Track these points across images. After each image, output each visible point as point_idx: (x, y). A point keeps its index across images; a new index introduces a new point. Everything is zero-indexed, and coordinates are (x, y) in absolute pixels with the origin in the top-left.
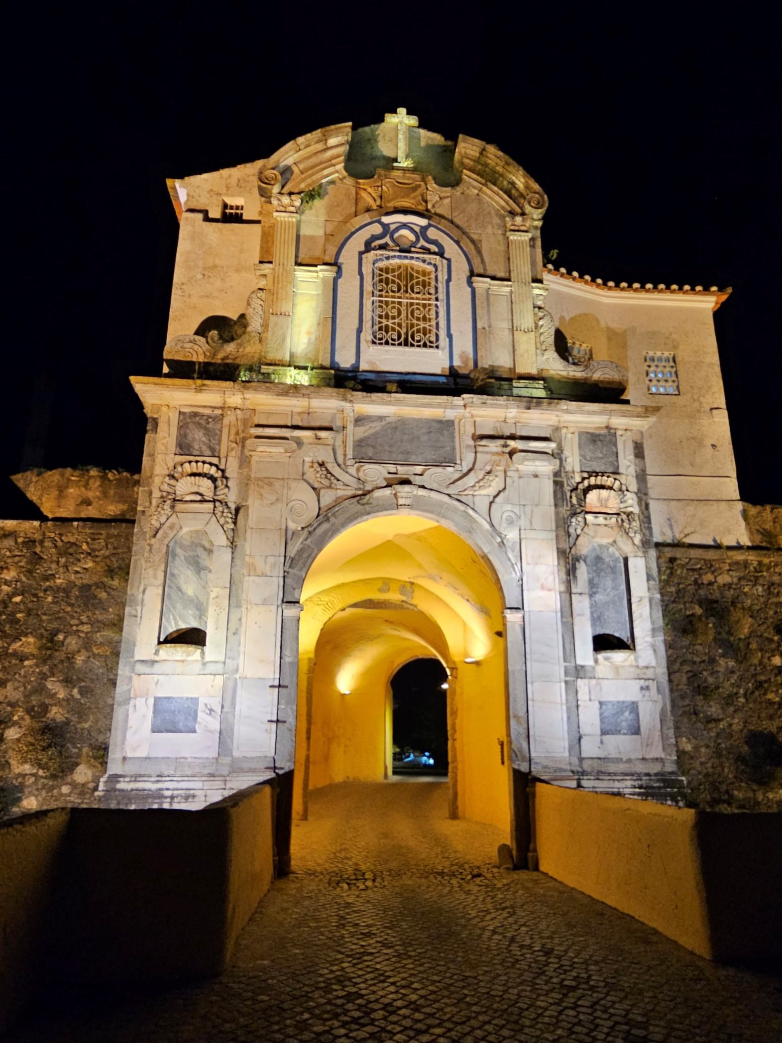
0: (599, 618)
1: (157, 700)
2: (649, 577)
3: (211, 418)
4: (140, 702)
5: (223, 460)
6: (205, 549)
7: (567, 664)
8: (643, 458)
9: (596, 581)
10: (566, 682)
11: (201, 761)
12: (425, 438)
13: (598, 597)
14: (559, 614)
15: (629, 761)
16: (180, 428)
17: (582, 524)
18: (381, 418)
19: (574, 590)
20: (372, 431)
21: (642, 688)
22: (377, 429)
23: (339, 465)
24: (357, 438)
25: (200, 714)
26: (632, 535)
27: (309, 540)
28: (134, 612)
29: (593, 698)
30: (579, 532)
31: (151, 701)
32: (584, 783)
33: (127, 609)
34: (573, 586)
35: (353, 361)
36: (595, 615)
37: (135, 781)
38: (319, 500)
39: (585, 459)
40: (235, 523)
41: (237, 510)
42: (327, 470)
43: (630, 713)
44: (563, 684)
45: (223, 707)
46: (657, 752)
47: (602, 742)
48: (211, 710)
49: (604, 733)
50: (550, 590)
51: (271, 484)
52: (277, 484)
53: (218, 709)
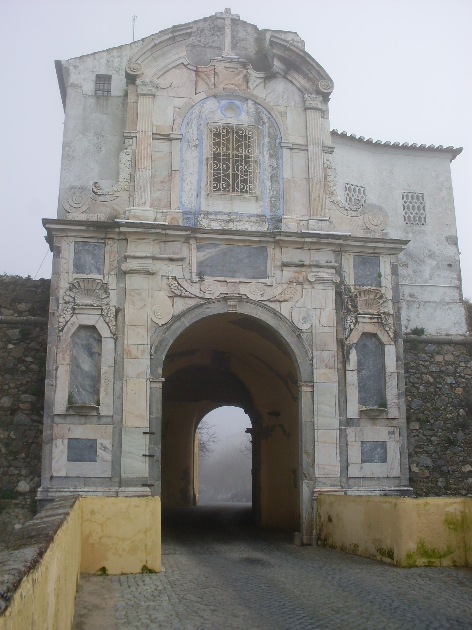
2: (398, 359)
3: (96, 246)
4: (59, 442)
5: (106, 277)
6: (95, 339)
7: (341, 418)
9: (363, 361)
10: (340, 430)
11: (100, 479)
13: (364, 372)
14: (337, 384)
16: (75, 253)
17: (354, 321)
19: (348, 368)
20: (210, 255)
22: (213, 254)
23: (186, 280)
25: (98, 450)
27: (167, 334)
28: (51, 382)
29: (357, 440)
30: (352, 327)
31: (66, 441)
33: (47, 381)
34: (347, 365)
36: (361, 385)
37: (60, 491)
38: (173, 305)
39: (358, 276)
41: (117, 312)
43: (381, 449)
44: (338, 431)
45: (113, 446)
46: (396, 472)
47: (361, 468)
49: (363, 461)
50: (331, 368)
53: (110, 447)
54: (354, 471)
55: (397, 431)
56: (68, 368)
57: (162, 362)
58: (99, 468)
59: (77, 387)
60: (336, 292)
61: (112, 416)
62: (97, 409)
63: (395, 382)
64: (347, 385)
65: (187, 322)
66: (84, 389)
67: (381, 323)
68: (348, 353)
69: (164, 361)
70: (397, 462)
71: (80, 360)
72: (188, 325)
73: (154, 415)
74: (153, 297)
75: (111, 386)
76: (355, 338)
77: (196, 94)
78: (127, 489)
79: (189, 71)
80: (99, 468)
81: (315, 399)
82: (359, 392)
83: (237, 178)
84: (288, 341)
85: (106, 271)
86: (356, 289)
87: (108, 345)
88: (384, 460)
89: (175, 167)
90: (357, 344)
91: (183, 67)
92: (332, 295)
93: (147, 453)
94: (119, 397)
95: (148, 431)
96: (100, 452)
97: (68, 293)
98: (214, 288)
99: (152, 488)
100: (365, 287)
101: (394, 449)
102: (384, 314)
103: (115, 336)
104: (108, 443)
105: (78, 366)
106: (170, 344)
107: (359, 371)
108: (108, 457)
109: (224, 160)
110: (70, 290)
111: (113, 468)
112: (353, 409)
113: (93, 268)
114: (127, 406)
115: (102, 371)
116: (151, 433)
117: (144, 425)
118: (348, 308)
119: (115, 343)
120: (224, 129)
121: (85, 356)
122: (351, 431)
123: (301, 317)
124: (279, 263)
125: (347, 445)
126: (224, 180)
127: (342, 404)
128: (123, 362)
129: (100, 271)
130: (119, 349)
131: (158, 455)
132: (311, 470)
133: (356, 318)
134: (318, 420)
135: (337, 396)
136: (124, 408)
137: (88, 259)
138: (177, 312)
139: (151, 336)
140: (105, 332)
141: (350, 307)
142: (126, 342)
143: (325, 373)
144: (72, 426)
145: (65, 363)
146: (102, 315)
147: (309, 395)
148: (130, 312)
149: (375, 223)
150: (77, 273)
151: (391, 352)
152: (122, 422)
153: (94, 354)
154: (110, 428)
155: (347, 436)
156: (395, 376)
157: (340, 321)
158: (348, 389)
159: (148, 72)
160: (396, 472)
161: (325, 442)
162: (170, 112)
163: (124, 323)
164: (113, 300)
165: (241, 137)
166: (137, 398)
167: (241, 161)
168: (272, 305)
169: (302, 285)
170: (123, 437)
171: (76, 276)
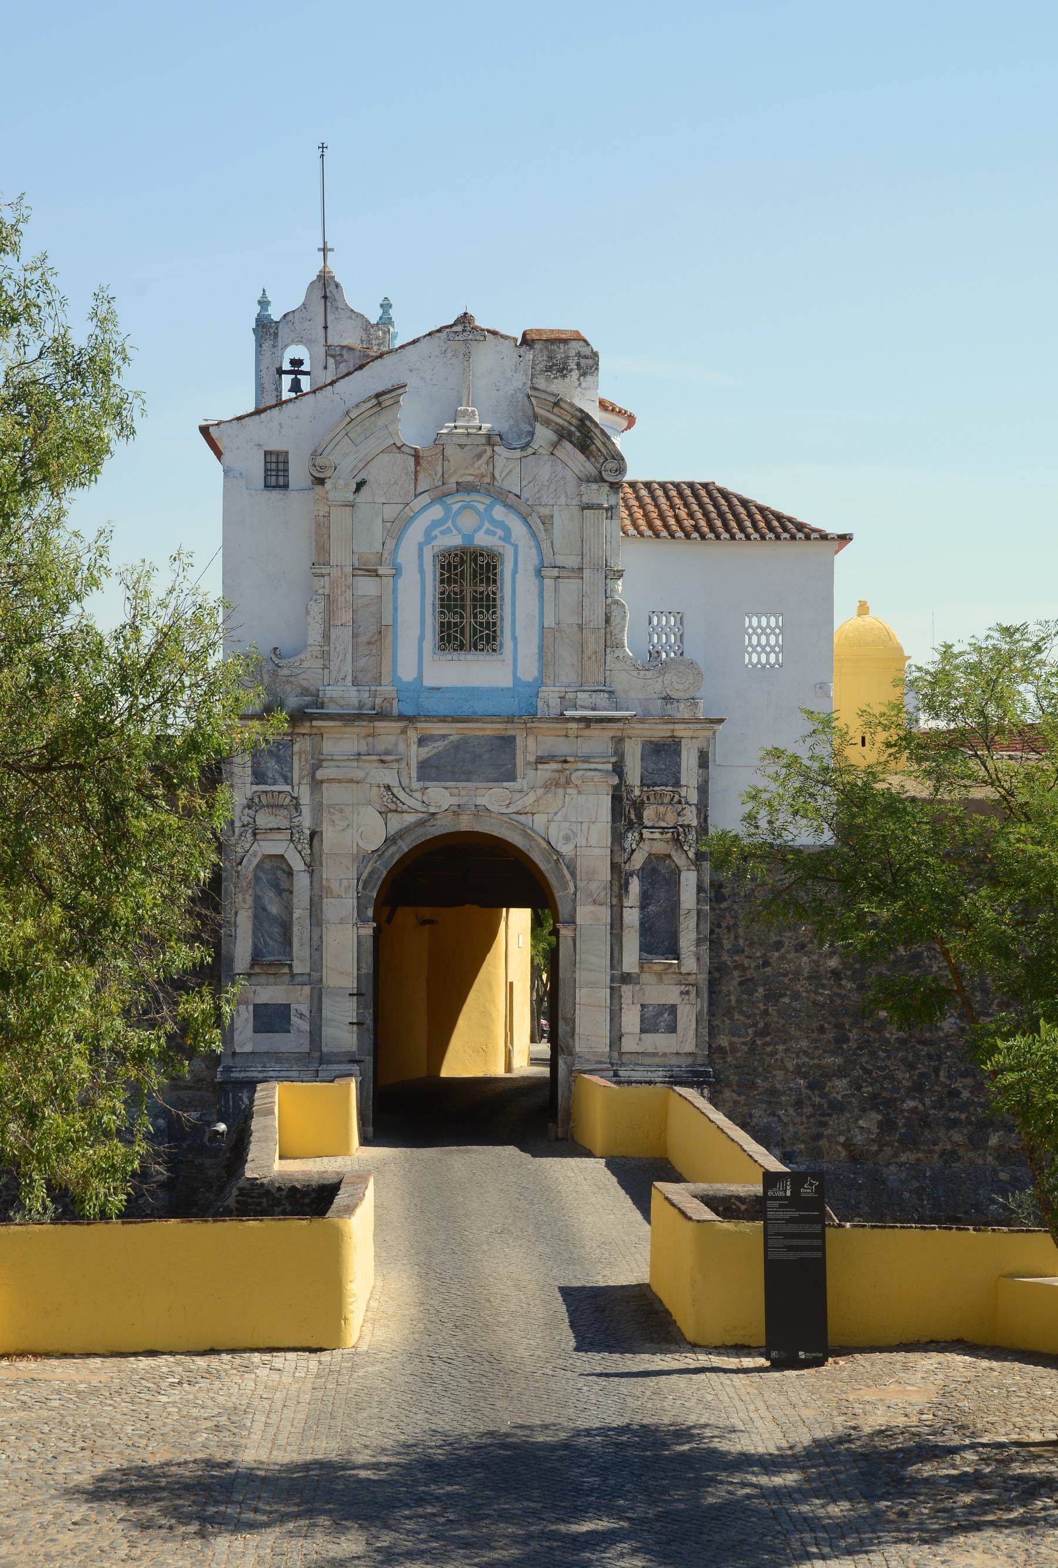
0: (650, 928)
1: (255, 1005)
2: (700, 889)
5: (296, 788)
6: (284, 872)
8: (707, 767)
9: (650, 892)
10: (612, 988)
12: (486, 756)
14: (609, 927)
15: (665, 1055)
17: (637, 838)
18: (444, 737)
19: (625, 904)
20: (436, 750)
21: (682, 993)
24: (421, 759)
26: (686, 848)
30: (634, 846)
31: (251, 1008)
32: (621, 1073)
34: (625, 900)
35: (415, 675)
39: (647, 770)
40: (311, 848)
42: (393, 794)
46: (689, 1046)
48: (301, 1014)
51: (341, 811)
52: (347, 810)
53: (307, 1014)
54: (629, 1044)
55: (693, 991)
56: (250, 913)
57: (373, 901)
58: (294, 1041)
59: (263, 936)
60: (613, 797)
61: (309, 974)
62: (290, 966)
63: (692, 922)
64: (624, 927)
65: (405, 846)
66: (271, 938)
67: (678, 839)
68: (627, 884)
69: (376, 900)
70: (691, 1033)
71: (266, 901)
72: (406, 850)
73: (364, 971)
74: (358, 814)
75: (307, 935)
76: (638, 861)
77: (416, 496)
78: (330, 1067)
79: (405, 457)
80: (294, 1041)
81: (578, 947)
82: (641, 935)
83: (475, 634)
84: (543, 868)
85: (296, 781)
86: (642, 791)
87: (302, 882)
88: (672, 1029)
89: (387, 620)
90: (642, 868)
91: (395, 450)
92: (607, 801)
93: (355, 1021)
94: (317, 949)
95: (355, 991)
96: (294, 1019)
97: (246, 811)
98: (441, 797)
99: (362, 1065)
100: (656, 788)
101: (688, 1016)
102: (681, 826)
103: (311, 868)
104: (304, 1008)
105: (264, 909)
106: (383, 876)
107: (643, 907)
108: (305, 1026)
109: (456, 606)
110: (249, 807)
111: (312, 1041)
112: (630, 961)
113: (277, 776)
114: (328, 959)
115: (295, 916)
116: (359, 994)
117: (350, 983)
118: (630, 820)
119: (311, 877)
120: (456, 555)
121: (272, 894)
122: (626, 990)
123: (562, 834)
124: (532, 759)
125: (621, 1009)
126: (456, 638)
127: (616, 954)
128: (321, 903)
129: (287, 780)
130: (316, 885)
131: (369, 1022)
132: (571, 1042)
133: (641, 834)
134: (581, 976)
135: (609, 943)
136: (324, 963)
137: (271, 765)
138: (392, 831)
139: (358, 867)
140: (297, 864)
141: (633, 817)
142: (324, 877)
143: (592, 912)
144: (258, 988)
145: (247, 906)
146: (291, 840)
147: (570, 942)
148: (330, 837)
149: (681, 687)
150: (257, 784)
151: (689, 880)
152: (321, 981)
153: (284, 892)
154: (307, 989)
155: (621, 997)
156: (694, 914)
157: (617, 837)
158: (625, 933)
159: (345, 461)
160: (689, 1046)
161: (589, 1005)
162: (378, 528)
163: (321, 850)
164: (306, 821)
165: (481, 566)
166: (341, 946)
167: (481, 606)
168: (522, 819)
169: (565, 788)
170: (324, 1000)
171: (255, 788)
